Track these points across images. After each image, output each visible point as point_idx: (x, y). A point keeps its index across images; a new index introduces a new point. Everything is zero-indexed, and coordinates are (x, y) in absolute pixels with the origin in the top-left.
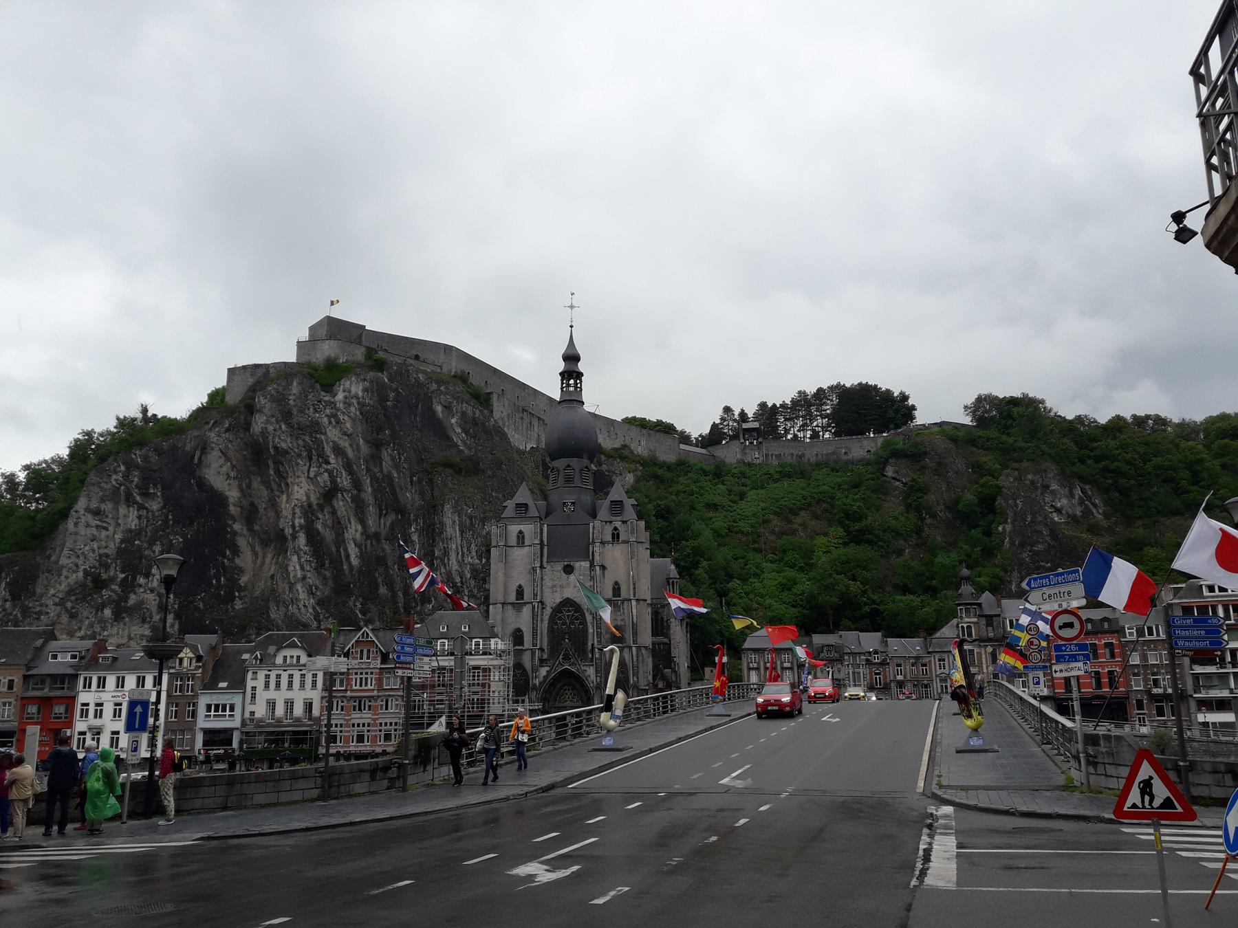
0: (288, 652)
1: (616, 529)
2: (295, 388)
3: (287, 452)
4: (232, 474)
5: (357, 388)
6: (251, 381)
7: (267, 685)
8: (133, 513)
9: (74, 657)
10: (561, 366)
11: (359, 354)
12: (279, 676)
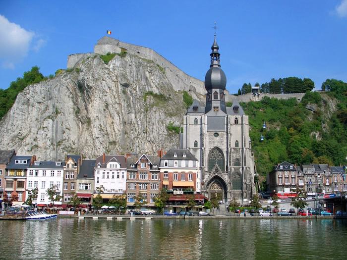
0: (112, 163)
1: (236, 119)
2: (95, 62)
3: (91, 88)
4: (71, 96)
5: (118, 63)
6: (77, 60)
7: (104, 176)
8: (35, 110)
9: (25, 162)
10: (211, 52)
11: (119, 51)
12: (108, 173)
